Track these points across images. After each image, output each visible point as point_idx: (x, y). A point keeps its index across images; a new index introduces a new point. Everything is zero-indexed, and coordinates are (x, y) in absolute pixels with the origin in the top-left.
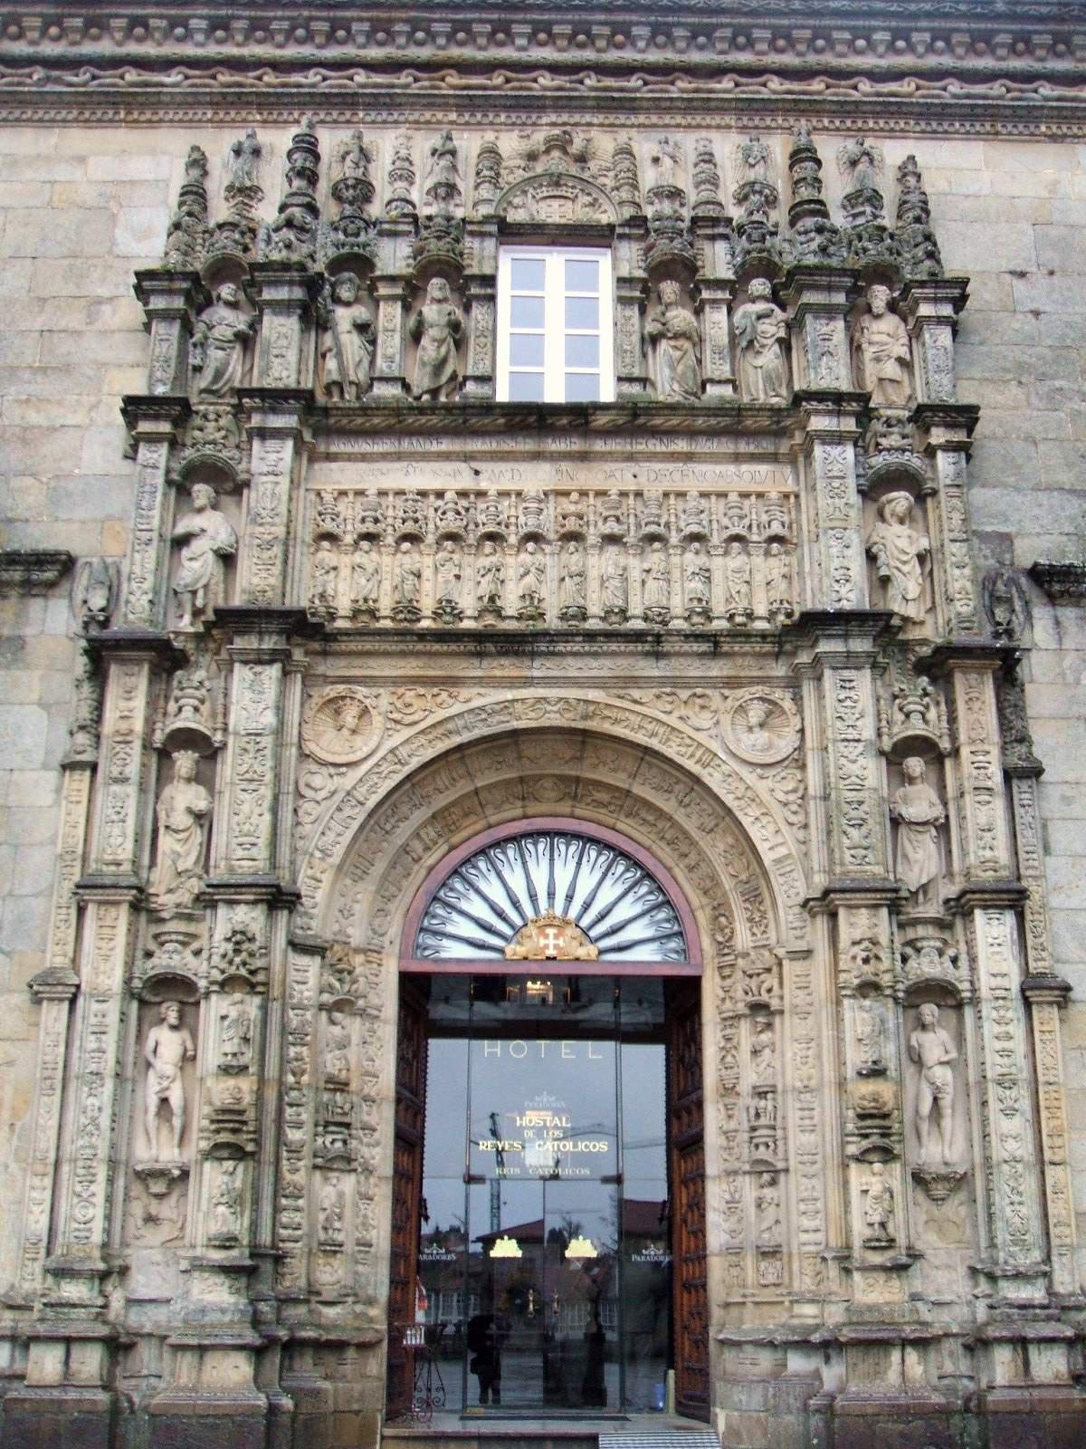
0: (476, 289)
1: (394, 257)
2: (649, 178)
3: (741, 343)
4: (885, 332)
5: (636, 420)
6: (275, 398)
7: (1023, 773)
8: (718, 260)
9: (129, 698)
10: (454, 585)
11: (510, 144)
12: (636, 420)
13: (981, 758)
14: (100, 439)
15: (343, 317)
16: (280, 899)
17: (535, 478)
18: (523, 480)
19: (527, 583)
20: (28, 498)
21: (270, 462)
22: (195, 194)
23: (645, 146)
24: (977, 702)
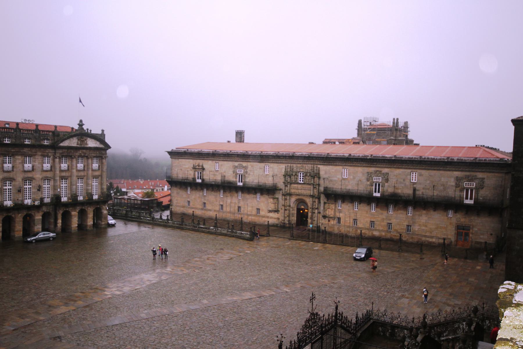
0: (298, 176)
1: (294, 174)
5: (304, 184)
7: (319, 202)
8: (308, 175)
9: (284, 197)
10: (297, 191)
11: (300, 165)
12: (304, 184)
13: (317, 202)
14: (282, 183)
16: (290, 206)
18: (300, 186)
19: (300, 191)
21: (289, 186)
22: (286, 169)
23: (306, 165)
24: (317, 200)
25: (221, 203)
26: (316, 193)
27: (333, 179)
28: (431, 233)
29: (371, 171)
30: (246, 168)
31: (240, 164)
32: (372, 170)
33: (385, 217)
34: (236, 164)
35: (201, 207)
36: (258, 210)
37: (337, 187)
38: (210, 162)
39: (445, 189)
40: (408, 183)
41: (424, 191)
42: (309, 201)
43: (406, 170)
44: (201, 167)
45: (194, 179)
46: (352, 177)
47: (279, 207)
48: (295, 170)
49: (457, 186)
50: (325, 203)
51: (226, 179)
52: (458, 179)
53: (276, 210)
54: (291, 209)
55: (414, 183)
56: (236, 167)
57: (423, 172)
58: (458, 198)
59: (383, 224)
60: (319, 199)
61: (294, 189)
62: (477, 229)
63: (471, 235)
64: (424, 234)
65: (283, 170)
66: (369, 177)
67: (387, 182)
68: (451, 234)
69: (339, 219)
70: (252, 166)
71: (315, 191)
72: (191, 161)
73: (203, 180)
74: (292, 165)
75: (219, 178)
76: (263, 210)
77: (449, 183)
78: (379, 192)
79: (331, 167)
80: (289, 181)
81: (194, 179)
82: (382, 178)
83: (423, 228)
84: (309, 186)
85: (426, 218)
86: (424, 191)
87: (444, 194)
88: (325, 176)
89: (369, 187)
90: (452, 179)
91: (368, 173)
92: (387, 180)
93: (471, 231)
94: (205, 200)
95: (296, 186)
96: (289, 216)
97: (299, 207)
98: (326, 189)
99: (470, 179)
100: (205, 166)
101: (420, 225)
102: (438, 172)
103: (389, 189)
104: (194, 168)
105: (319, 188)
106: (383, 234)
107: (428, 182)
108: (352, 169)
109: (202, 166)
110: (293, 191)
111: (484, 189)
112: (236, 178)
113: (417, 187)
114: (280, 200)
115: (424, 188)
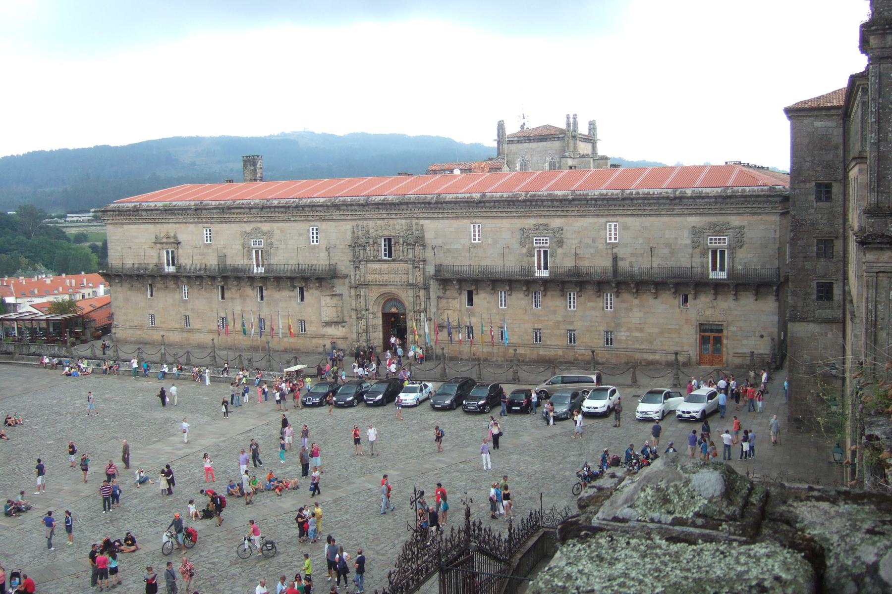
1: (371, 242)
2: (397, 227)
3: (403, 252)
4: (416, 249)
6: (361, 260)
8: (401, 241)
10: (379, 278)
11: (382, 223)
13: (422, 298)
14: (349, 263)
15: (368, 248)
17: (386, 266)
20: (343, 268)
21: (362, 267)
22: (353, 232)
23: (395, 222)
25: (223, 315)
26: (420, 280)
27: (452, 247)
28: (651, 343)
29: (527, 226)
30: (268, 234)
31: (256, 228)
32: (530, 222)
33: (560, 319)
34: (248, 227)
35: (178, 326)
36: (302, 322)
37: (462, 262)
38: (192, 227)
39: (672, 252)
40: (601, 247)
41: (633, 259)
42: (407, 297)
43: (595, 220)
44: (172, 240)
45: (159, 267)
46: (490, 241)
47: (345, 313)
48: (372, 232)
49: (695, 245)
50: (439, 298)
51: (229, 261)
52: (696, 232)
53: (339, 319)
54: (371, 316)
55: (614, 246)
56: (249, 234)
57: (629, 220)
58: (697, 270)
59: (557, 332)
60: (426, 288)
61: (374, 271)
62: (734, 329)
63: (725, 341)
64: (637, 346)
65: (349, 235)
66: (525, 236)
67: (561, 246)
68: (688, 342)
69: (470, 330)
70: (282, 231)
71: (418, 274)
72: (150, 227)
73: (179, 267)
74: (365, 223)
75: (212, 261)
76: (311, 322)
77: (680, 242)
78: (546, 268)
79: (446, 221)
80: (362, 257)
81: (159, 267)
82: (551, 239)
83: (637, 334)
84: (405, 265)
85: (641, 315)
86: (633, 259)
87: (671, 263)
88: (436, 242)
89: (525, 259)
90: (686, 233)
91: (521, 229)
92: (560, 243)
93: (725, 332)
94: (187, 309)
95: (377, 266)
96: (366, 331)
97: (387, 311)
98: (439, 269)
99: (718, 230)
100: (181, 237)
101: (629, 329)
102: (658, 219)
103: (564, 261)
104: (158, 242)
105: (424, 268)
106: (560, 352)
107: (641, 241)
108: (489, 224)
109: (175, 237)
110: (371, 277)
111: (745, 247)
112: (250, 258)
113: (621, 252)
114: (346, 297)
115: (632, 255)
